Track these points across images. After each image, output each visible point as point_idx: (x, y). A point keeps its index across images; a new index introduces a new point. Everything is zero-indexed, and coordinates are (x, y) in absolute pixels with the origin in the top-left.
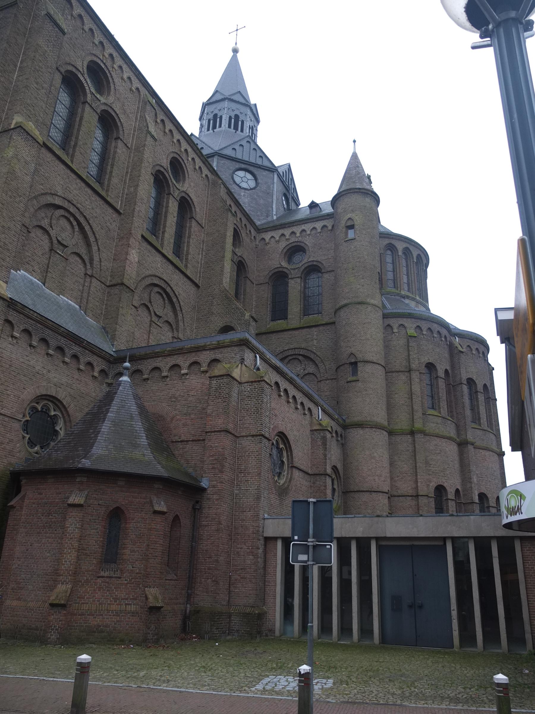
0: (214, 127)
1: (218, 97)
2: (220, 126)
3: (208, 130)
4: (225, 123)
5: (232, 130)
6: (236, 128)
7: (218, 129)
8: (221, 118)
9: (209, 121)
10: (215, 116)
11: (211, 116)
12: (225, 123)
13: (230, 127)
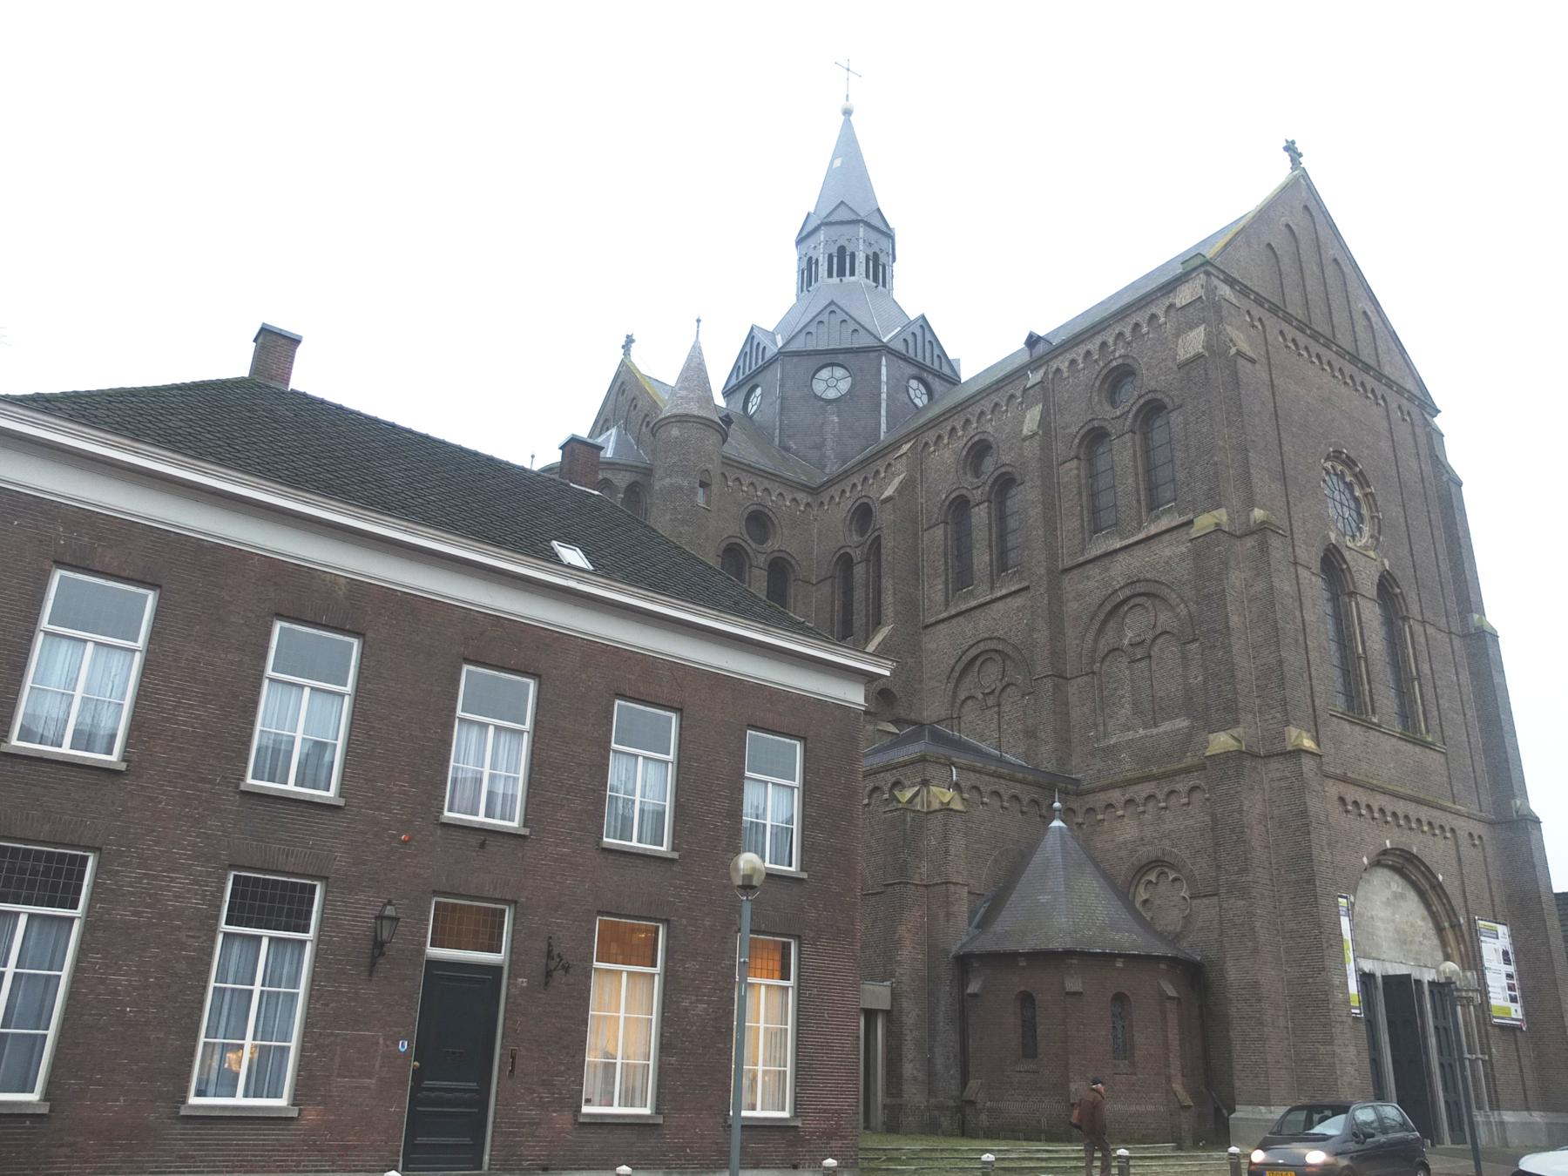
0: (841, 273)
1: (843, 214)
2: (852, 273)
3: (830, 275)
4: (860, 267)
5: (871, 283)
6: (876, 280)
7: (847, 279)
8: (853, 256)
9: (830, 257)
10: (842, 250)
11: (834, 250)
12: (860, 267)
13: (867, 276)
